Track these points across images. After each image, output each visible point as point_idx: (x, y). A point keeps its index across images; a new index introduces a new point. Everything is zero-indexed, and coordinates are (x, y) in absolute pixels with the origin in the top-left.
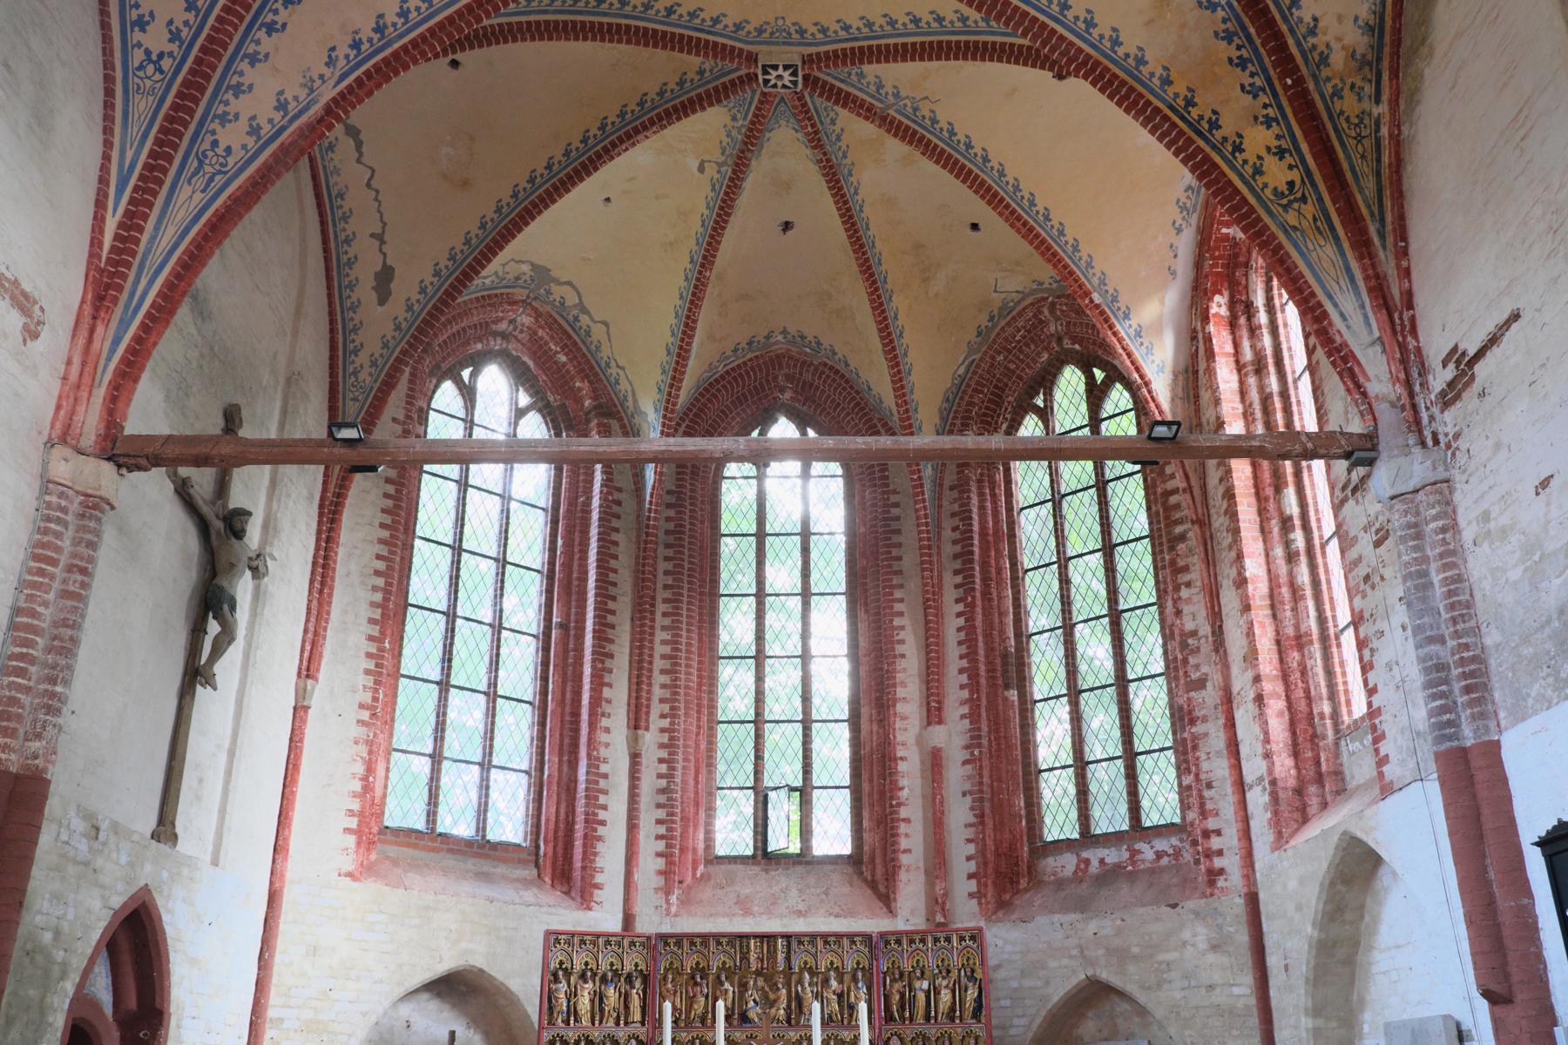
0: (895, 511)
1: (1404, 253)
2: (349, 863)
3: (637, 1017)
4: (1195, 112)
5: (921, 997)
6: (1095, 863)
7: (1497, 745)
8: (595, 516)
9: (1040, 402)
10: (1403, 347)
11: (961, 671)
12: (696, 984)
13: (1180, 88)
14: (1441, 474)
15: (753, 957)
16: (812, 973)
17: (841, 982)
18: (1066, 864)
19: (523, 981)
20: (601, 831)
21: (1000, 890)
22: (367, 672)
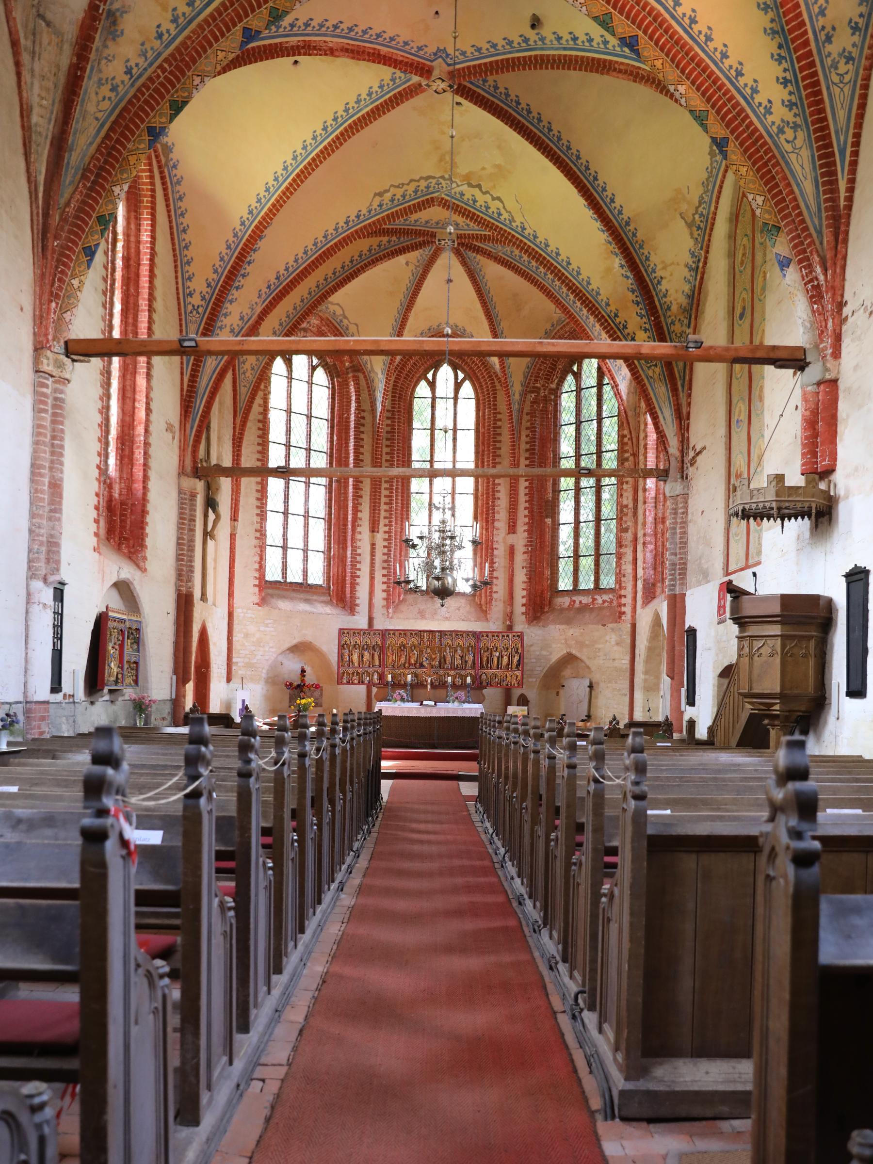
0: (499, 423)
1: (689, 395)
2: (256, 599)
3: (377, 663)
4: (618, 320)
5: (495, 659)
6: (577, 602)
7: (685, 595)
8: (352, 425)
9: (575, 368)
10: (683, 435)
11: (525, 508)
13: (613, 308)
14: (686, 491)
18: (565, 601)
19: (330, 649)
20: (358, 580)
21: (535, 611)
22: (257, 515)
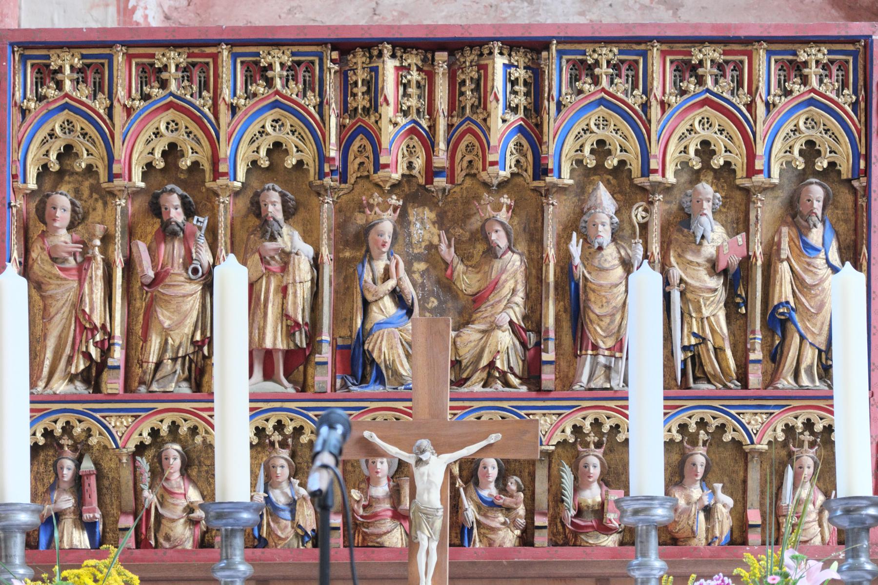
12: (167, 232)
15: (390, 125)
16: (629, 187)
17: (740, 223)
